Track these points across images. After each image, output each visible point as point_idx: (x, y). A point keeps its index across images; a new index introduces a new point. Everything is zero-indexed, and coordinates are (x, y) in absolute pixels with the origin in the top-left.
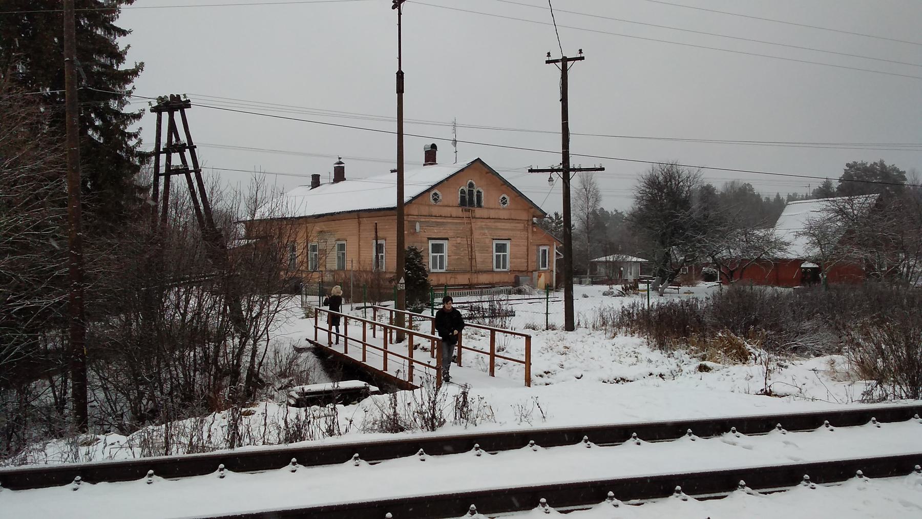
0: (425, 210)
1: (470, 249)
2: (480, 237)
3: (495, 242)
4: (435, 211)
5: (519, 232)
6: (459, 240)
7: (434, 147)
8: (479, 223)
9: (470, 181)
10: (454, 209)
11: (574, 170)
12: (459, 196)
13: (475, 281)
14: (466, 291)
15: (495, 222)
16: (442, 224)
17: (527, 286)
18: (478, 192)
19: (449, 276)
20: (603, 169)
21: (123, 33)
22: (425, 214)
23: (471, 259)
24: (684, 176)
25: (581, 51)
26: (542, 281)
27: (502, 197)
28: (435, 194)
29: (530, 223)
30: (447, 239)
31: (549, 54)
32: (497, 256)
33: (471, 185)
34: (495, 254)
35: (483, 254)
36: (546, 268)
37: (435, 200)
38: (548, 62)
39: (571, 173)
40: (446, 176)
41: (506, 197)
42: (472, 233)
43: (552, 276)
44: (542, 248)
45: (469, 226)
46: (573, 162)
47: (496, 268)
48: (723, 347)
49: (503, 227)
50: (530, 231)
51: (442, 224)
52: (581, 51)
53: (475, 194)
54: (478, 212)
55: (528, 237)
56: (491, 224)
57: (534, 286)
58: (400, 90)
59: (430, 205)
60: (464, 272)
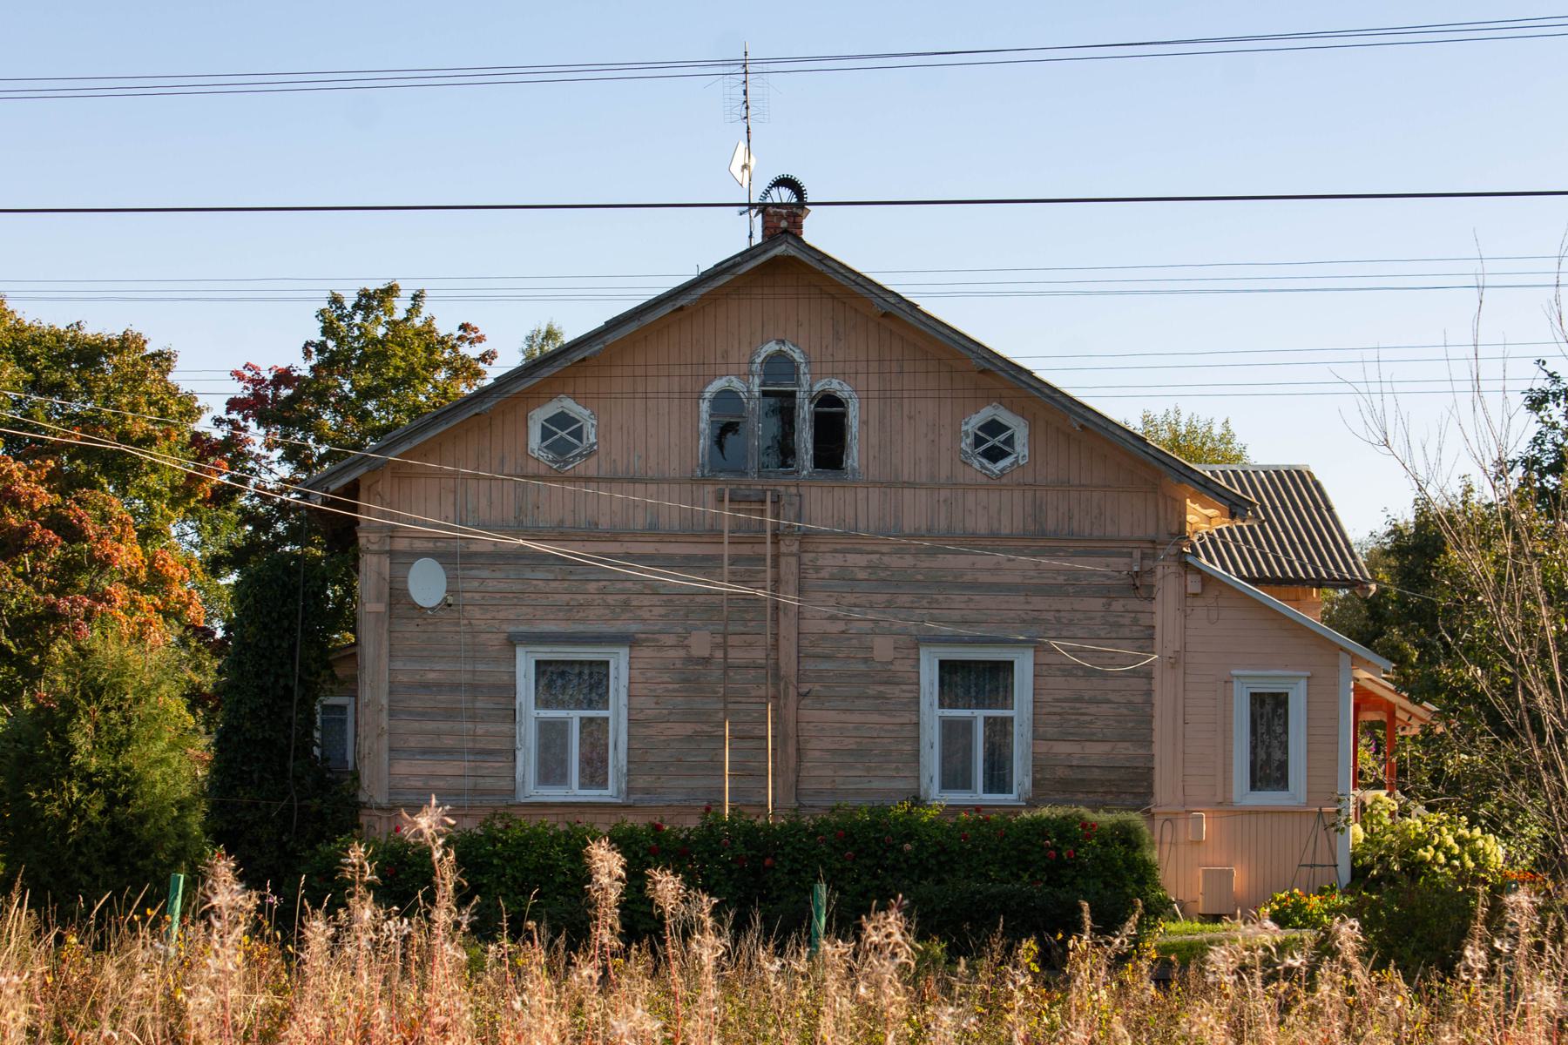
5: (1097, 604)
9: (772, 347)
18: (829, 399)
28: (562, 420)
33: (780, 366)
34: (932, 715)
37: (560, 450)
40: (597, 322)
41: (1005, 417)
47: (945, 785)
49: (985, 578)
53: (805, 411)
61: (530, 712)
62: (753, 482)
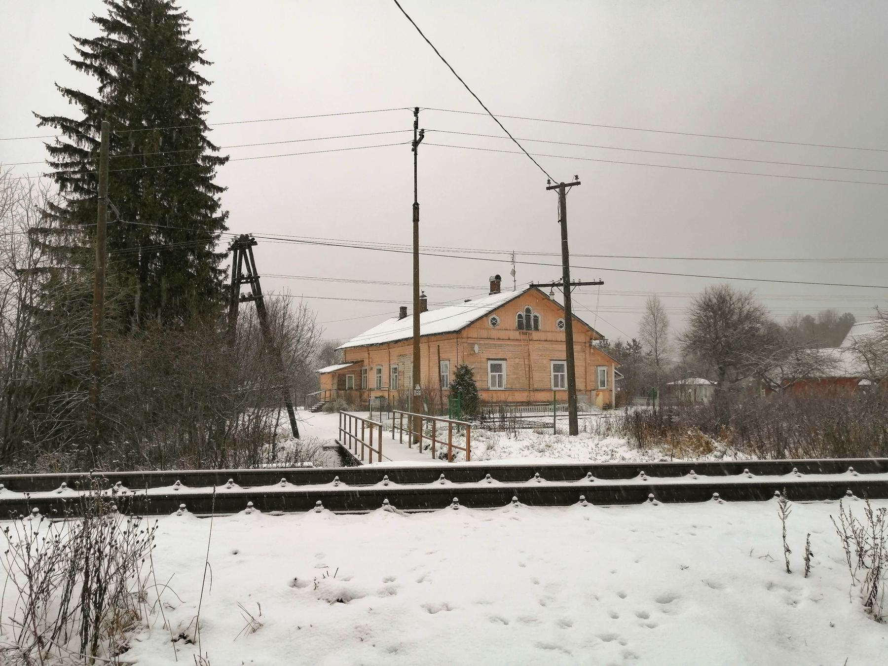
0: (484, 333)
1: (527, 369)
2: (538, 358)
3: (552, 363)
4: (494, 334)
6: (517, 360)
7: (498, 277)
8: (537, 345)
10: (512, 332)
11: (574, 284)
12: (517, 321)
13: (532, 399)
14: (523, 408)
15: (552, 344)
16: (500, 346)
17: (584, 404)
18: (535, 316)
19: (507, 393)
20: (601, 283)
21: (220, 190)
22: (483, 337)
23: (530, 378)
24: (734, 299)
25: (577, 177)
26: (600, 400)
27: (559, 321)
29: (587, 345)
30: (505, 359)
31: (549, 182)
32: (555, 376)
33: (528, 311)
35: (541, 374)
36: (605, 388)
37: (494, 324)
38: (548, 188)
39: (572, 288)
42: (529, 355)
43: (611, 395)
44: (600, 369)
45: (527, 348)
46: (574, 277)
47: (554, 387)
48: (691, 445)
49: (560, 349)
50: (587, 352)
51: (500, 346)
52: (577, 177)
53: (532, 318)
54: (535, 335)
55: (585, 358)
56: (547, 345)
57: (591, 403)
58: (416, 220)
59: (487, 329)
60: (523, 390)
61: (490, 374)
62: (525, 331)
